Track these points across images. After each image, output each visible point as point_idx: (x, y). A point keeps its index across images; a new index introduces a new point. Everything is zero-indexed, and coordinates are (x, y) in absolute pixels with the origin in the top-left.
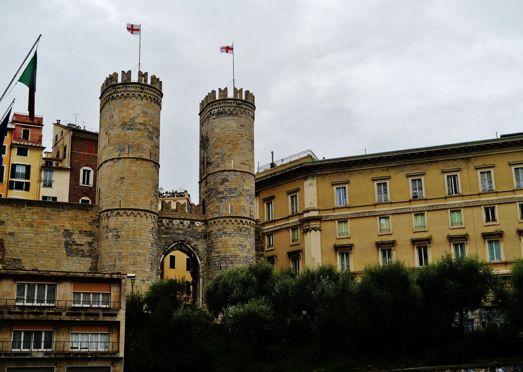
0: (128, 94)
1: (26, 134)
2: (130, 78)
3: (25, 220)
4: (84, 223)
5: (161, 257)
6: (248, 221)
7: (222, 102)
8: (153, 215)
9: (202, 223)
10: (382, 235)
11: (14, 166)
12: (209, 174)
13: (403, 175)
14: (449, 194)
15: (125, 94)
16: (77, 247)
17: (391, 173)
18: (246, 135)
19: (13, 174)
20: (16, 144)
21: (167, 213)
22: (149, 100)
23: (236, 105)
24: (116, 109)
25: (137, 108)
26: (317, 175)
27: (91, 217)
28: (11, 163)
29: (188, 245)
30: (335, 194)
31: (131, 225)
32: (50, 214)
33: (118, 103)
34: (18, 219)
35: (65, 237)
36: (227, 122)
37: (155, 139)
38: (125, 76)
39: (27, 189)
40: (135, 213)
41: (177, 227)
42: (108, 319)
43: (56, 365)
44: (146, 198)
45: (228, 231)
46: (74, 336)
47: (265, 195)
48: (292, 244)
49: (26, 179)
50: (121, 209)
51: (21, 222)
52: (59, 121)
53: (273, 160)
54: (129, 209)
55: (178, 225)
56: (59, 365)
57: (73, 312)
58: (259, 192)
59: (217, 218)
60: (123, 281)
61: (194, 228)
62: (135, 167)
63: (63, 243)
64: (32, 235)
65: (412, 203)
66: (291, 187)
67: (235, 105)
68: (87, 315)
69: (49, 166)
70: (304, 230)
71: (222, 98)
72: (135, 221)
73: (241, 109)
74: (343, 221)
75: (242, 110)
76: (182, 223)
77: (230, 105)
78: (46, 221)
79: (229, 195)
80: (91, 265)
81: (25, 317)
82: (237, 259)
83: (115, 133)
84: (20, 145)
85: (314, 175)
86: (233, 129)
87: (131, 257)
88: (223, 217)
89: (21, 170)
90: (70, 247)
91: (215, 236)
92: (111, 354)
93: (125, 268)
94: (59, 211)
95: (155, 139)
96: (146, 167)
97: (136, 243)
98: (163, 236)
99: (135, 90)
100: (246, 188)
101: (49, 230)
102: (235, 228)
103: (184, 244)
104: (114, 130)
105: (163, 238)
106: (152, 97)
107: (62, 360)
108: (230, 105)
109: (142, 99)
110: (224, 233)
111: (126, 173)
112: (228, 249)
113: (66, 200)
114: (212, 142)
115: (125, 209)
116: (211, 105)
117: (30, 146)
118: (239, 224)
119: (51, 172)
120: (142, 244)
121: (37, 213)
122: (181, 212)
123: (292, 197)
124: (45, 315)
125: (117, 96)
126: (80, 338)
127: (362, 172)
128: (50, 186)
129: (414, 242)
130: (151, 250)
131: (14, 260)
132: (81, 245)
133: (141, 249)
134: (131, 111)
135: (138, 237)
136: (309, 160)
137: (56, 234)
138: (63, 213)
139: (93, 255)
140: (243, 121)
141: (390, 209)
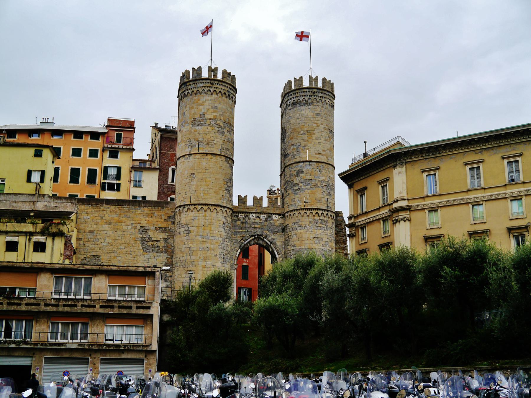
0: (198, 90)
1: (119, 137)
2: (200, 74)
3: (104, 218)
4: (159, 220)
6: (325, 213)
7: (297, 91)
8: (224, 210)
9: (280, 216)
11: (106, 168)
12: (286, 167)
13: (498, 157)
15: (195, 90)
16: (152, 243)
17: (484, 156)
18: (322, 124)
19: (105, 177)
20: (108, 147)
21: (243, 207)
22: (220, 95)
23: (312, 94)
24: (188, 106)
25: (206, 104)
26: (406, 162)
27: (166, 214)
29: (265, 239)
30: (425, 182)
31: (201, 220)
32: (127, 212)
33: (189, 99)
34: (97, 218)
35: (141, 234)
36: (302, 112)
37: (226, 133)
38: (195, 72)
39: (118, 190)
40: (205, 208)
41: (253, 221)
42: (141, 312)
43: (90, 355)
44: (216, 193)
45: (303, 223)
46: (109, 328)
47: (358, 186)
48: (383, 236)
49: (117, 180)
50: (191, 205)
51: (100, 221)
52: (156, 124)
53: (366, 150)
54: (199, 204)
55: (255, 219)
56: (93, 356)
57: (107, 304)
58: (353, 183)
59: (292, 211)
60: (157, 274)
61: (271, 222)
62: (205, 162)
63: (140, 239)
64: (111, 232)
65: (508, 187)
66: (381, 176)
67: (310, 93)
68: (120, 307)
69: (140, 167)
70: (393, 221)
71: (297, 87)
72: (205, 216)
73: (317, 98)
74: (433, 210)
75: (318, 99)
76: (258, 217)
77: (305, 94)
78: (124, 219)
79: (304, 187)
80: (166, 261)
81: (61, 309)
83: (186, 130)
84: (111, 148)
85: (402, 163)
86: (308, 118)
87: (201, 252)
88: (298, 210)
89: (112, 172)
90: (146, 243)
91: (291, 229)
92: (143, 346)
93: (195, 263)
94: (135, 209)
95: (226, 133)
96: (216, 162)
97: (205, 238)
98: (238, 231)
99: (205, 85)
100: (322, 178)
101: (126, 227)
102: (310, 220)
103: (261, 239)
104: (186, 127)
105: (239, 232)
106: (223, 92)
107: (96, 351)
108: (305, 94)
109: (212, 94)
111: (196, 168)
112: (303, 242)
113: (155, 198)
114: (288, 134)
115: (195, 205)
116: (287, 95)
117: (120, 148)
118: (314, 216)
119: (141, 172)
120: (212, 238)
121: (115, 211)
122: (258, 205)
123: (383, 187)
124: (79, 308)
125: (188, 93)
126: (115, 330)
127: (453, 156)
128: (140, 186)
129: (510, 230)
130: (223, 245)
131: (94, 256)
133: (211, 244)
134: (201, 107)
135: (207, 231)
136: (398, 147)
137: (133, 231)
138: (139, 211)
139: (169, 250)
140: (319, 110)
141: (483, 195)
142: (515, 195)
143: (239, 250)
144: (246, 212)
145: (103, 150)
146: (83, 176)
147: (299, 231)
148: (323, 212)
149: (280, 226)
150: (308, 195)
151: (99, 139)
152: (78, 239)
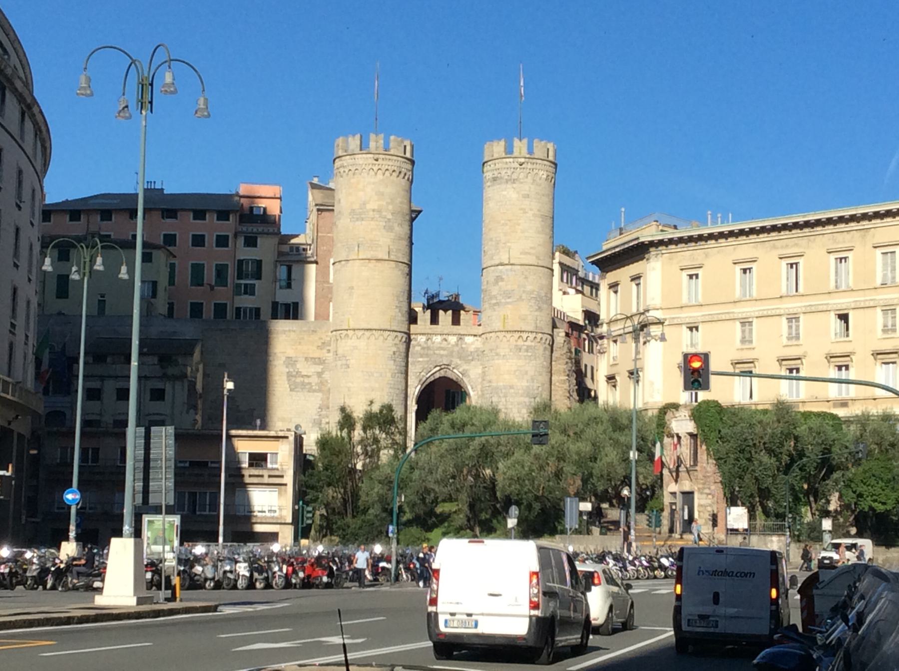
6: (532, 336)
10: (742, 349)
11: (240, 262)
14: (836, 287)
15: (353, 169)
18: (531, 210)
28: (237, 258)
29: (455, 370)
40: (368, 333)
76: (446, 340)
79: (503, 301)
82: (512, 391)
90: (293, 379)
100: (529, 288)
110: (497, 354)
115: (354, 330)
123: (638, 285)
132: (308, 377)
134: (361, 194)
141: (754, 309)
142: (791, 311)
145: (236, 236)
146: (210, 275)
151: (228, 220)
152: (205, 375)
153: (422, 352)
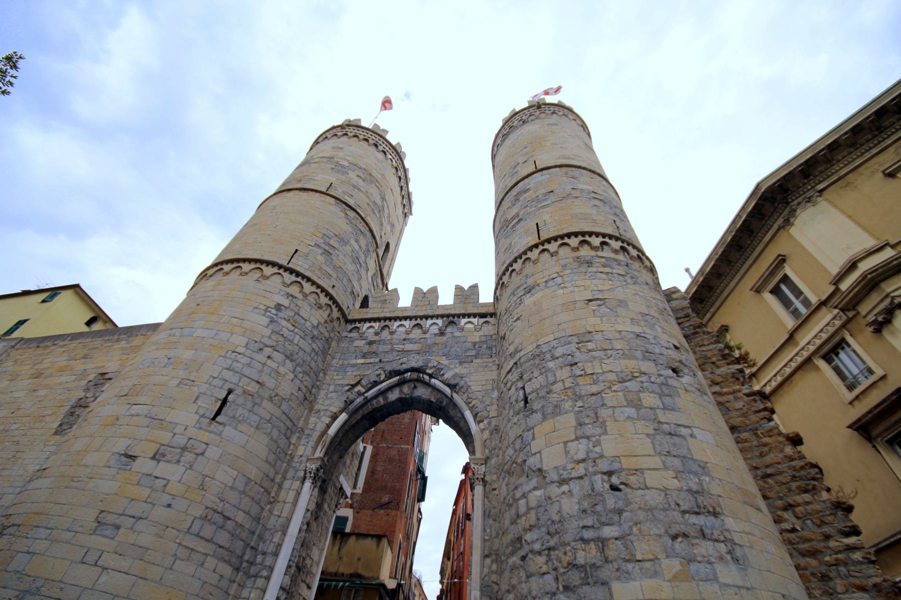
5: (334, 417)
6: (617, 245)
41: (404, 336)
61: (457, 334)
82: (590, 346)
98: (353, 362)
102: (563, 262)
105: (353, 366)
106: (361, 137)
118: (576, 249)
120: (206, 333)
123: (776, 291)
143: (343, 417)
144: (385, 319)
147: (528, 300)
148: (607, 240)
149: (485, 342)
150: (546, 217)
153: (366, 349)
